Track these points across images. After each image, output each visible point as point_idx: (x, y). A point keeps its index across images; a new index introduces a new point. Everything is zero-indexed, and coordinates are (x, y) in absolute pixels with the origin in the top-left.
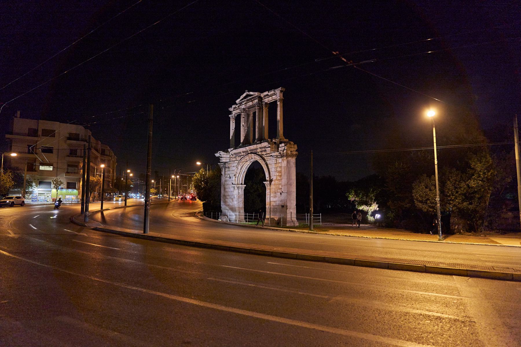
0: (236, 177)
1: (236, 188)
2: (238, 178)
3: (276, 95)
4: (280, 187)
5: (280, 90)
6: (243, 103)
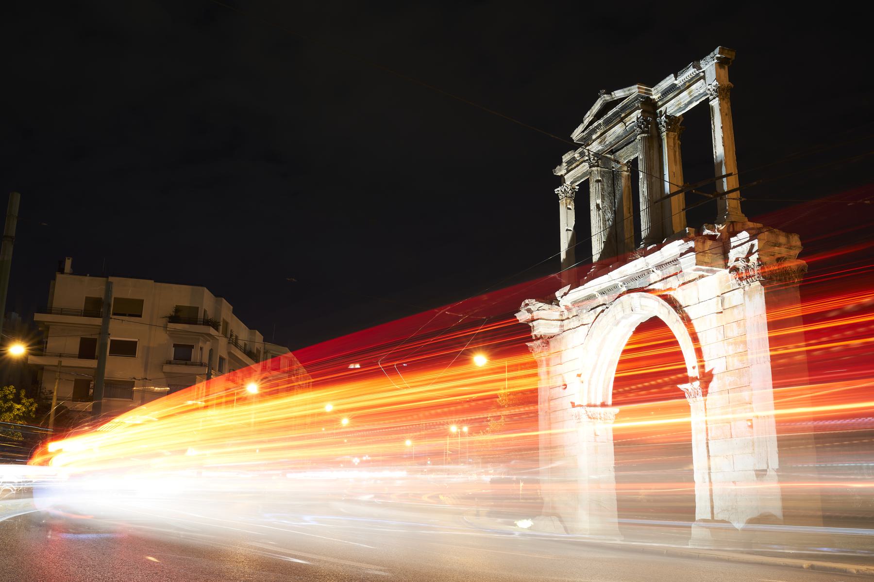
1: (584, 418)
2: (589, 384)
3: (704, 78)
5: (717, 58)
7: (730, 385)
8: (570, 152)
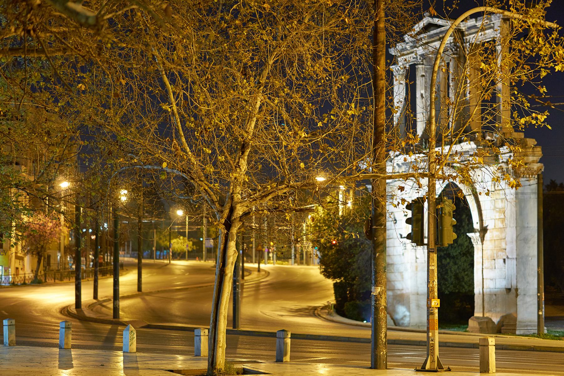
4: (503, 246)
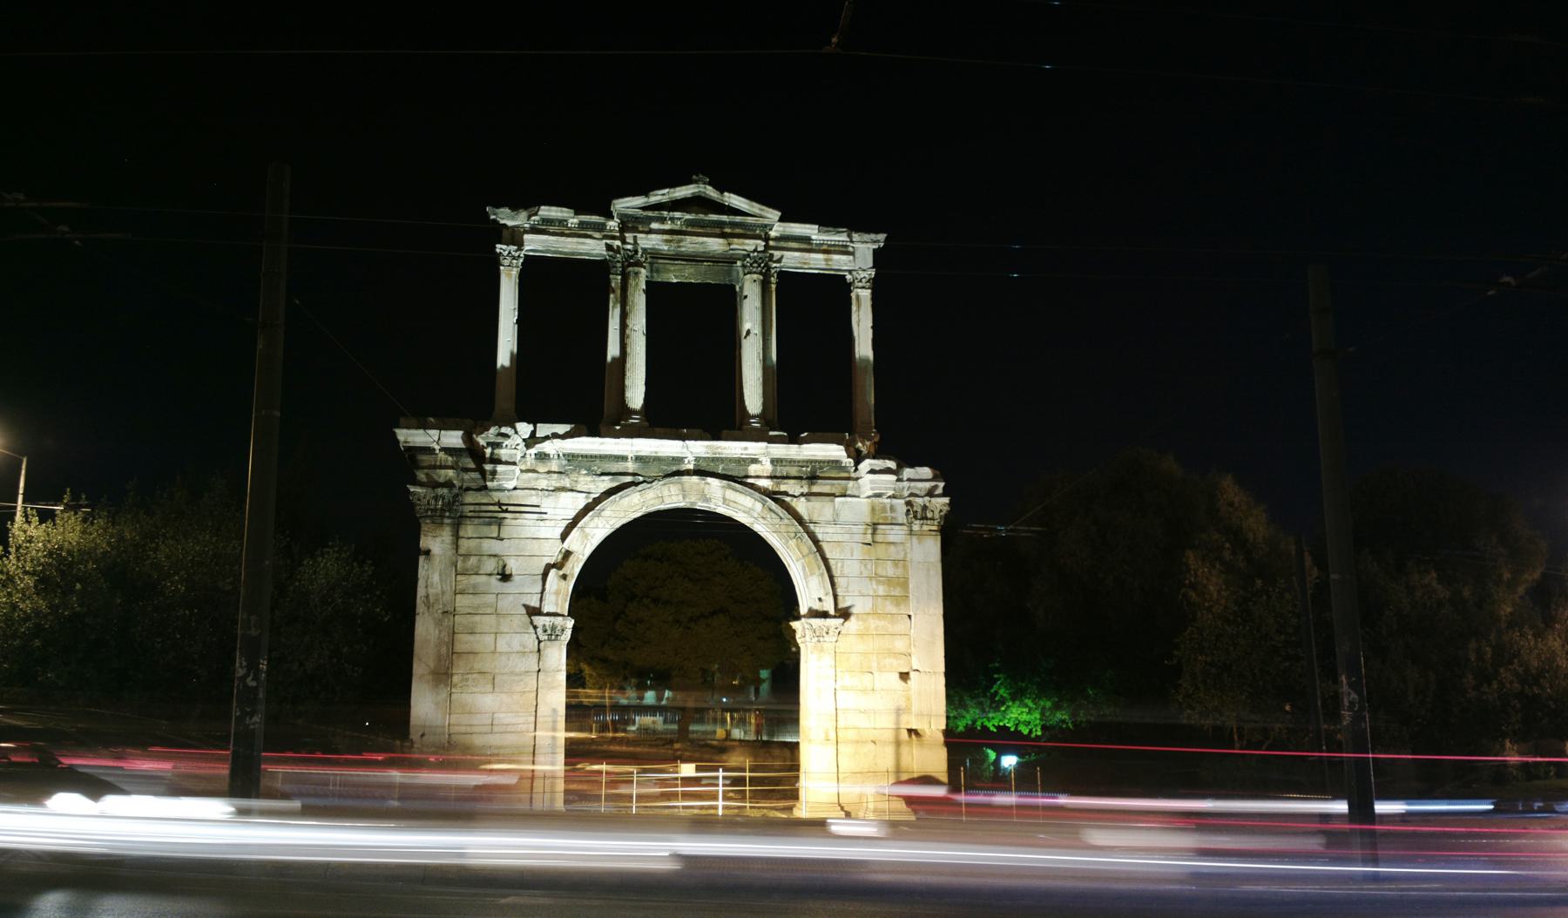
0: (564, 577)
4: (900, 645)
6: (654, 226)
7: (876, 628)
8: (564, 209)
